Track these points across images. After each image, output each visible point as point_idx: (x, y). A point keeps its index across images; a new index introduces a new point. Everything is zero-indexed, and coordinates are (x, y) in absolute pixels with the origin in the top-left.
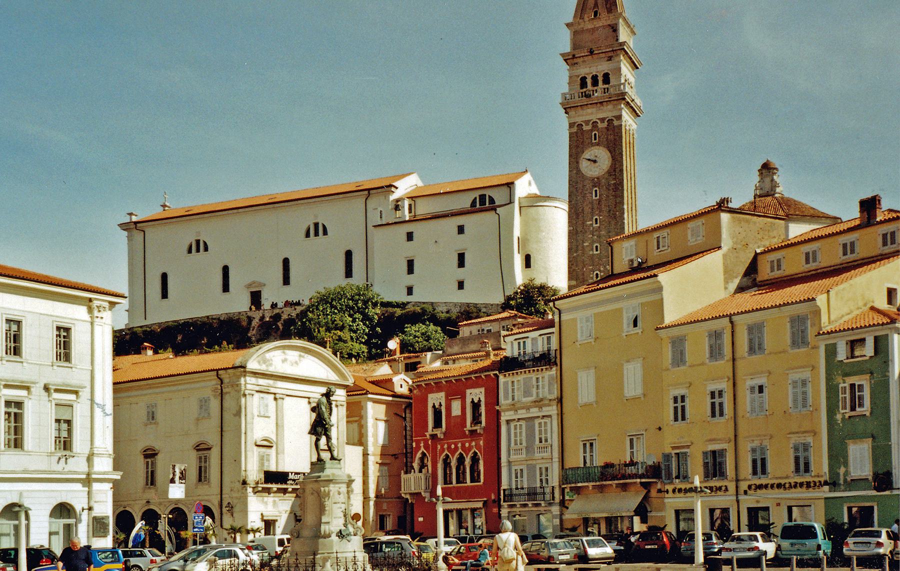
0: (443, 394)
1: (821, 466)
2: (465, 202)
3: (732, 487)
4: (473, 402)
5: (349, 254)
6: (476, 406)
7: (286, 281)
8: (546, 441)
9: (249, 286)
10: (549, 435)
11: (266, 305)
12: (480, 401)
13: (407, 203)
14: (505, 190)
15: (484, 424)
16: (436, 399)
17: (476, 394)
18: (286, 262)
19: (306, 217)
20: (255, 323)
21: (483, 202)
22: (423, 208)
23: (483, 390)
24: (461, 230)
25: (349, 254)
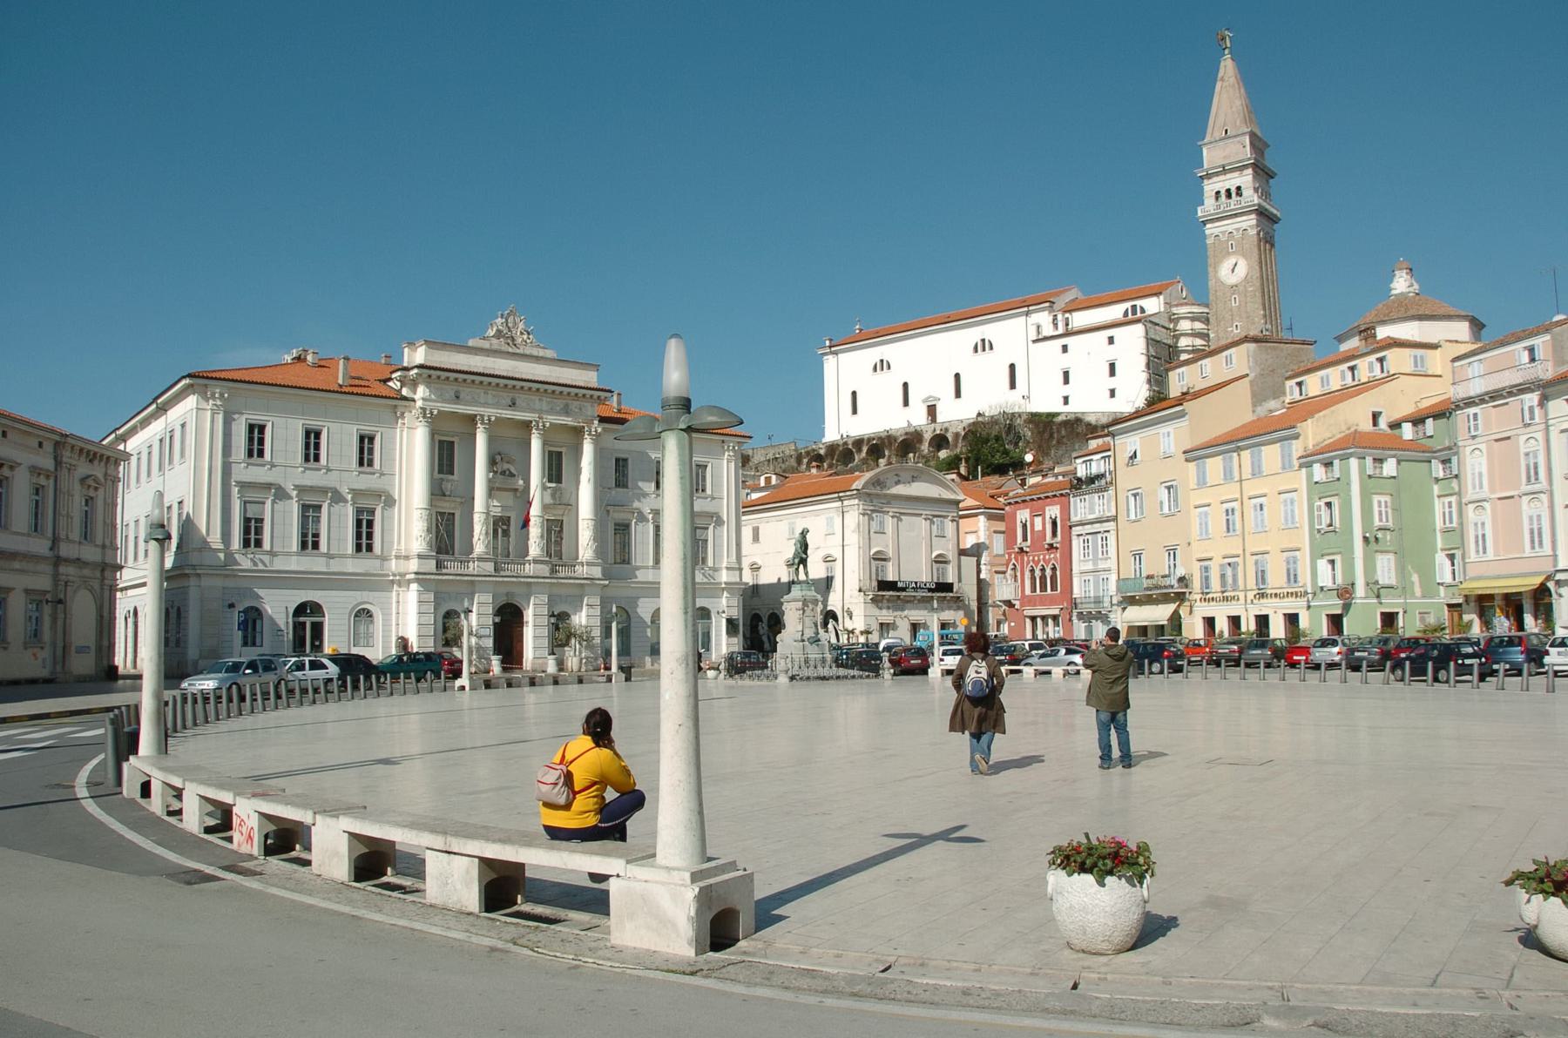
1: (1305, 578)
3: (1241, 595)
5: (1012, 367)
6: (1054, 523)
7: (958, 394)
9: (924, 401)
11: (940, 419)
14: (1154, 299)
16: (1023, 515)
17: (1053, 511)
18: (957, 376)
19: (973, 334)
20: (928, 436)
21: (1134, 313)
24: (1111, 340)
25: (1012, 367)
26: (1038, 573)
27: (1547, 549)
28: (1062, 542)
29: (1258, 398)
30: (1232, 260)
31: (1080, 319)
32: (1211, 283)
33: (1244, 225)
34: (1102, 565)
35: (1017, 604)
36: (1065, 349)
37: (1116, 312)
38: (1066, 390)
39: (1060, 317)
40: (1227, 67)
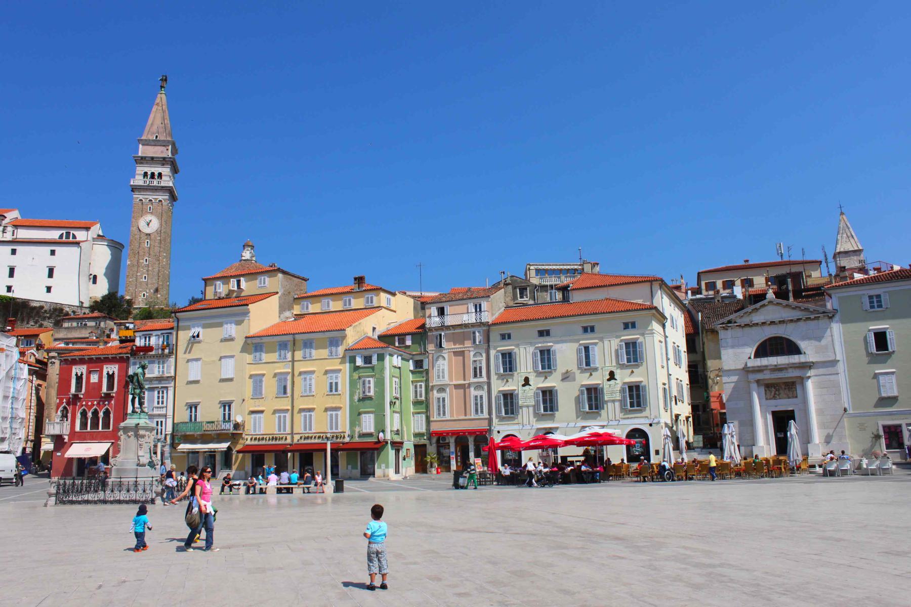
0: (85, 367)
2: (54, 235)
4: (108, 374)
8: (163, 403)
10: (165, 400)
12: (113, 374)
13: (10, 229)
15: (115, 389)
21: (68, 237)
22: (23, 234)
23: (117, 366)
24: (53, 253)
26: (90, 415)
27: (486, 415)
28: (116, 393)
29: (282, 309)
30: (149, 217)
31: (23, 234)
32: (134, 229)
33: (160, 198)
34: (156, 412)
35: (66, 438)
36: (14, 252)
37: (54, 235)
38: (10, 282)
39: (10, 229)
40: (162, 98)
